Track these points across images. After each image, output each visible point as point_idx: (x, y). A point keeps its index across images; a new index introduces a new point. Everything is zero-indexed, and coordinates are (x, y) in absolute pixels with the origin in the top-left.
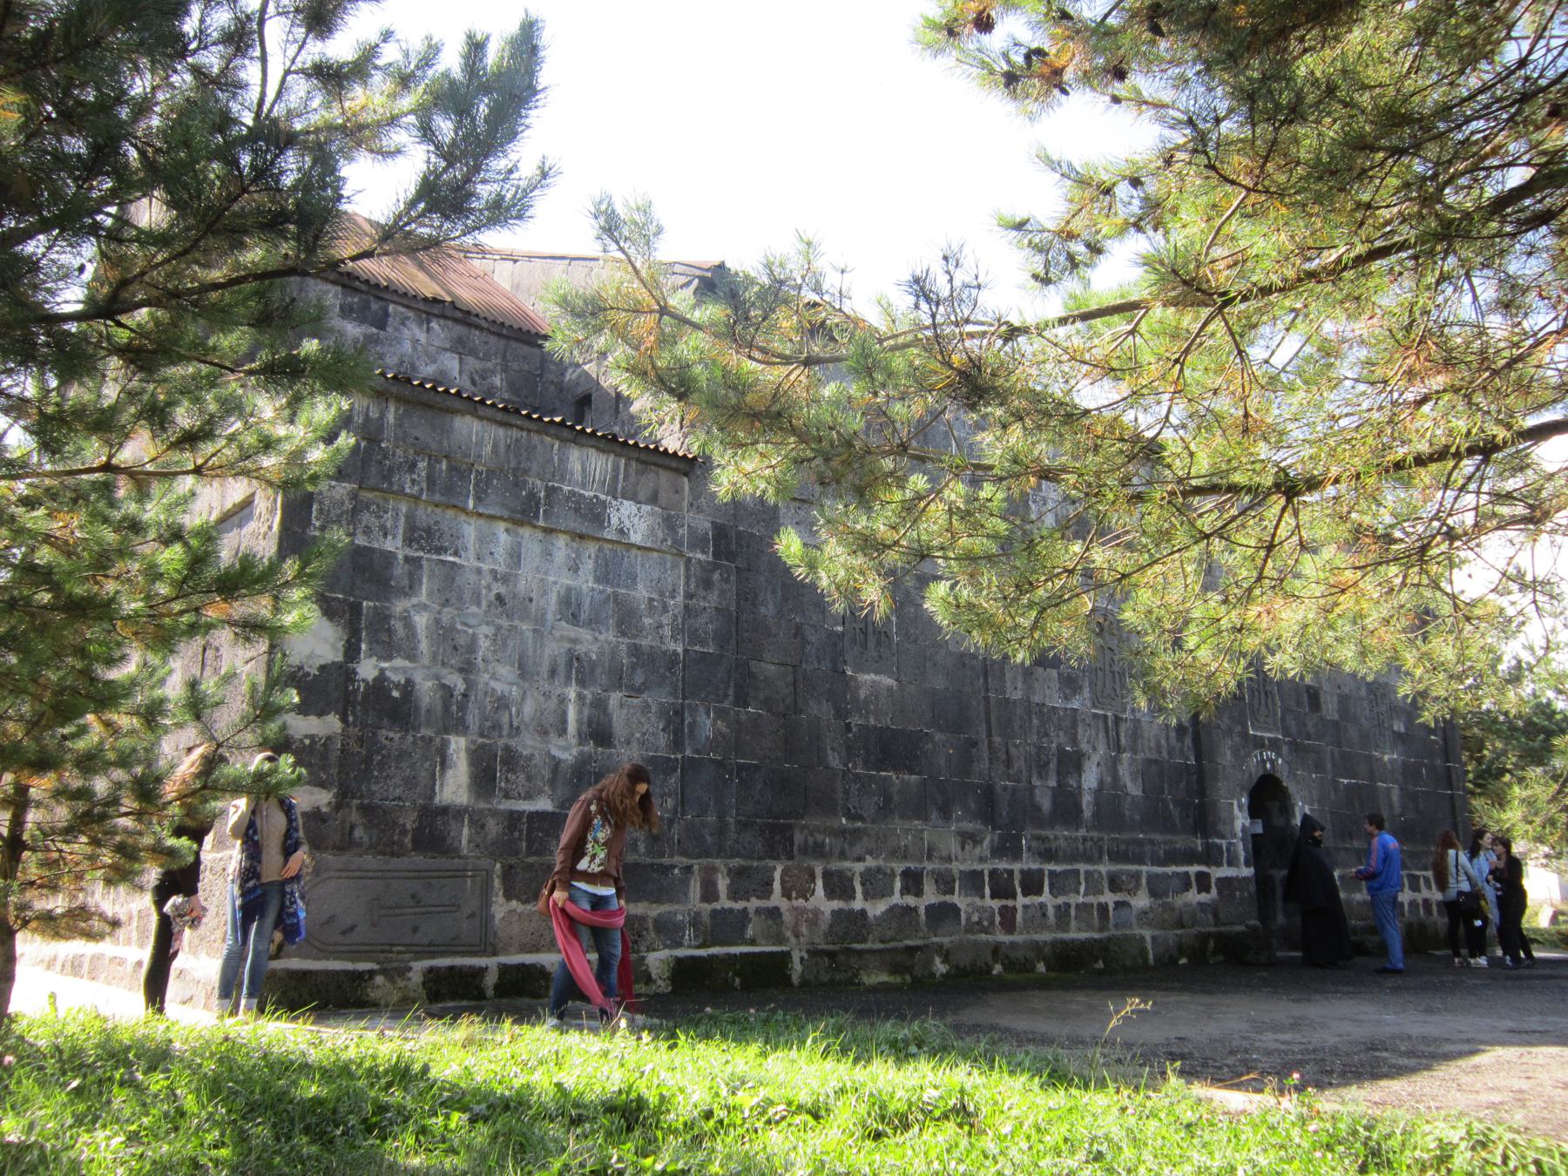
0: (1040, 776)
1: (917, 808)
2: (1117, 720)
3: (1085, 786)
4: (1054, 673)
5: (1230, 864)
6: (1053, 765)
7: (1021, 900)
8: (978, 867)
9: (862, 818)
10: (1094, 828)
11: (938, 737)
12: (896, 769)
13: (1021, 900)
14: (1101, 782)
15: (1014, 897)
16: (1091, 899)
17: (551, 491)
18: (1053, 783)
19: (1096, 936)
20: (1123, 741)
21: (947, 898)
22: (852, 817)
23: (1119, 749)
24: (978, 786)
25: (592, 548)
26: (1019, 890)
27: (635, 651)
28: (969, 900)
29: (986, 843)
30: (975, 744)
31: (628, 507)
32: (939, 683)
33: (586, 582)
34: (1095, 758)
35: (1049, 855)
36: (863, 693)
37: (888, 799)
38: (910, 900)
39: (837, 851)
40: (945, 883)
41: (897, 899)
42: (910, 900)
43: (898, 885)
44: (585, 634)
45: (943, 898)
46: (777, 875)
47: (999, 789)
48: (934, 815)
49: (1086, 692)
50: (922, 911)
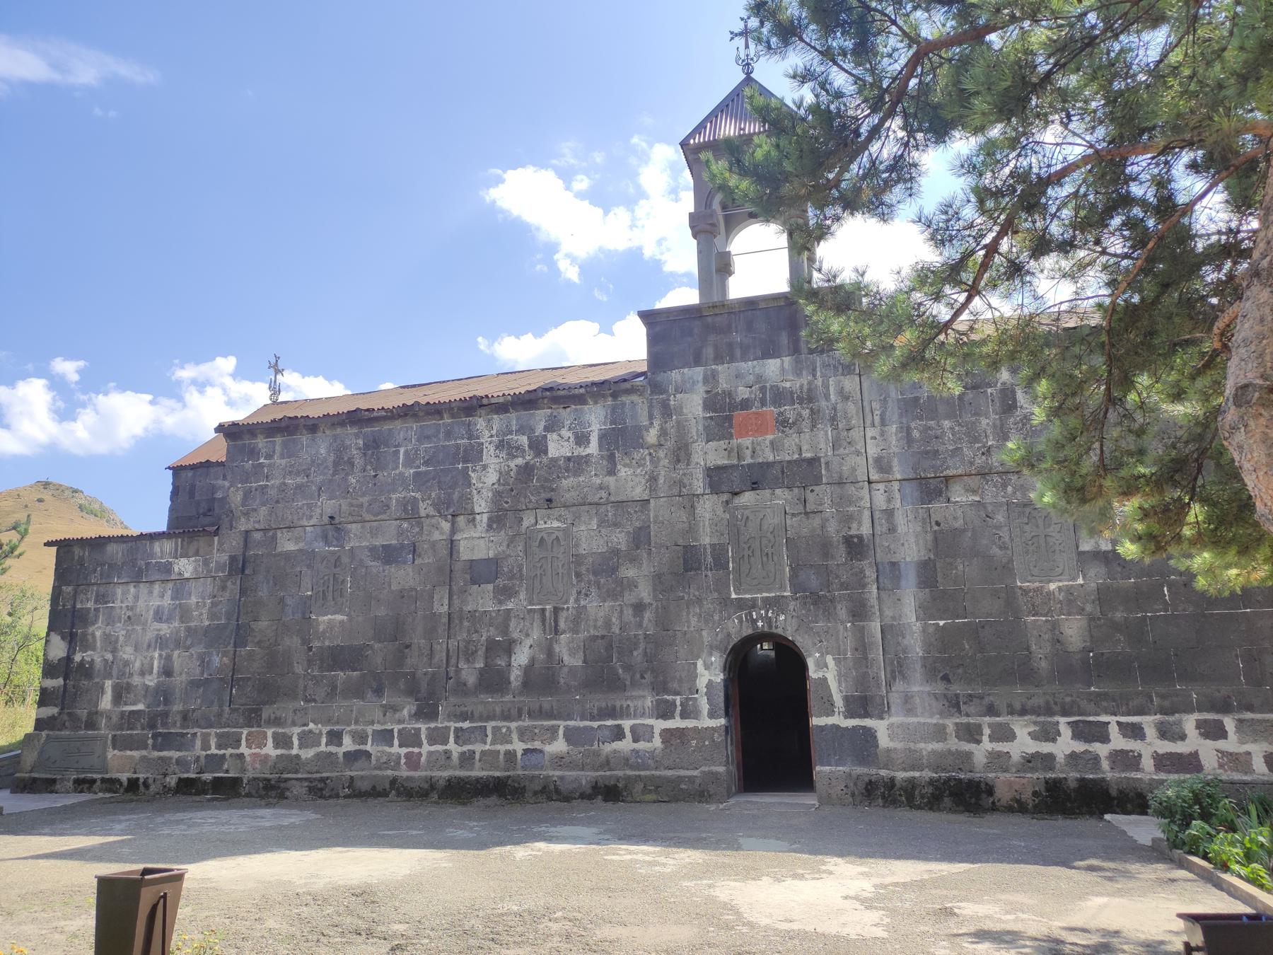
0: (468, 661)
1: (356, 691)
2: (556, 611)
3: (514, 664)
4: (490, 587)
5: (684, 716)
6: (481, 653)
7: (426, 748)
8: (389, 727)
9: (315, 701)
10: (520, 694)
11: (377, 646)
12: (342, 670)
13: (426, 748)
14: (533, 660)
15: (420, 745)
16: (502, 748)
17: (148, 564)
18: (480, 664)
19: (497, 774)
20: (562, 625)
21: (362, 747)
22: (307, 701)
23: (556, 632)
24: (407, 674)
25: (170, 585)
26: (425, 742)
27: (188, 629)
28: (380, 748)
29: (405, 712)
30: (408, 647)
31: (183, 561)
32: (381, 612)
33: (167, 601)
34: (529, 642)
35: (464, 717)
36: (321, 628)
37: (334, 688)
38: (332, 749)
39: (289, 722)
40: (360, 738)
41: (323, 748)
42: (332, 749)
43: (324, 740)
44: (164, 626)
45: (358, 747)
46: (244, 737)
47: (419, 673)
48: (369, 695)
49: (522, 596)
50: (341, 755)
